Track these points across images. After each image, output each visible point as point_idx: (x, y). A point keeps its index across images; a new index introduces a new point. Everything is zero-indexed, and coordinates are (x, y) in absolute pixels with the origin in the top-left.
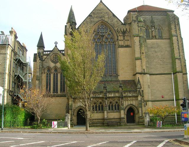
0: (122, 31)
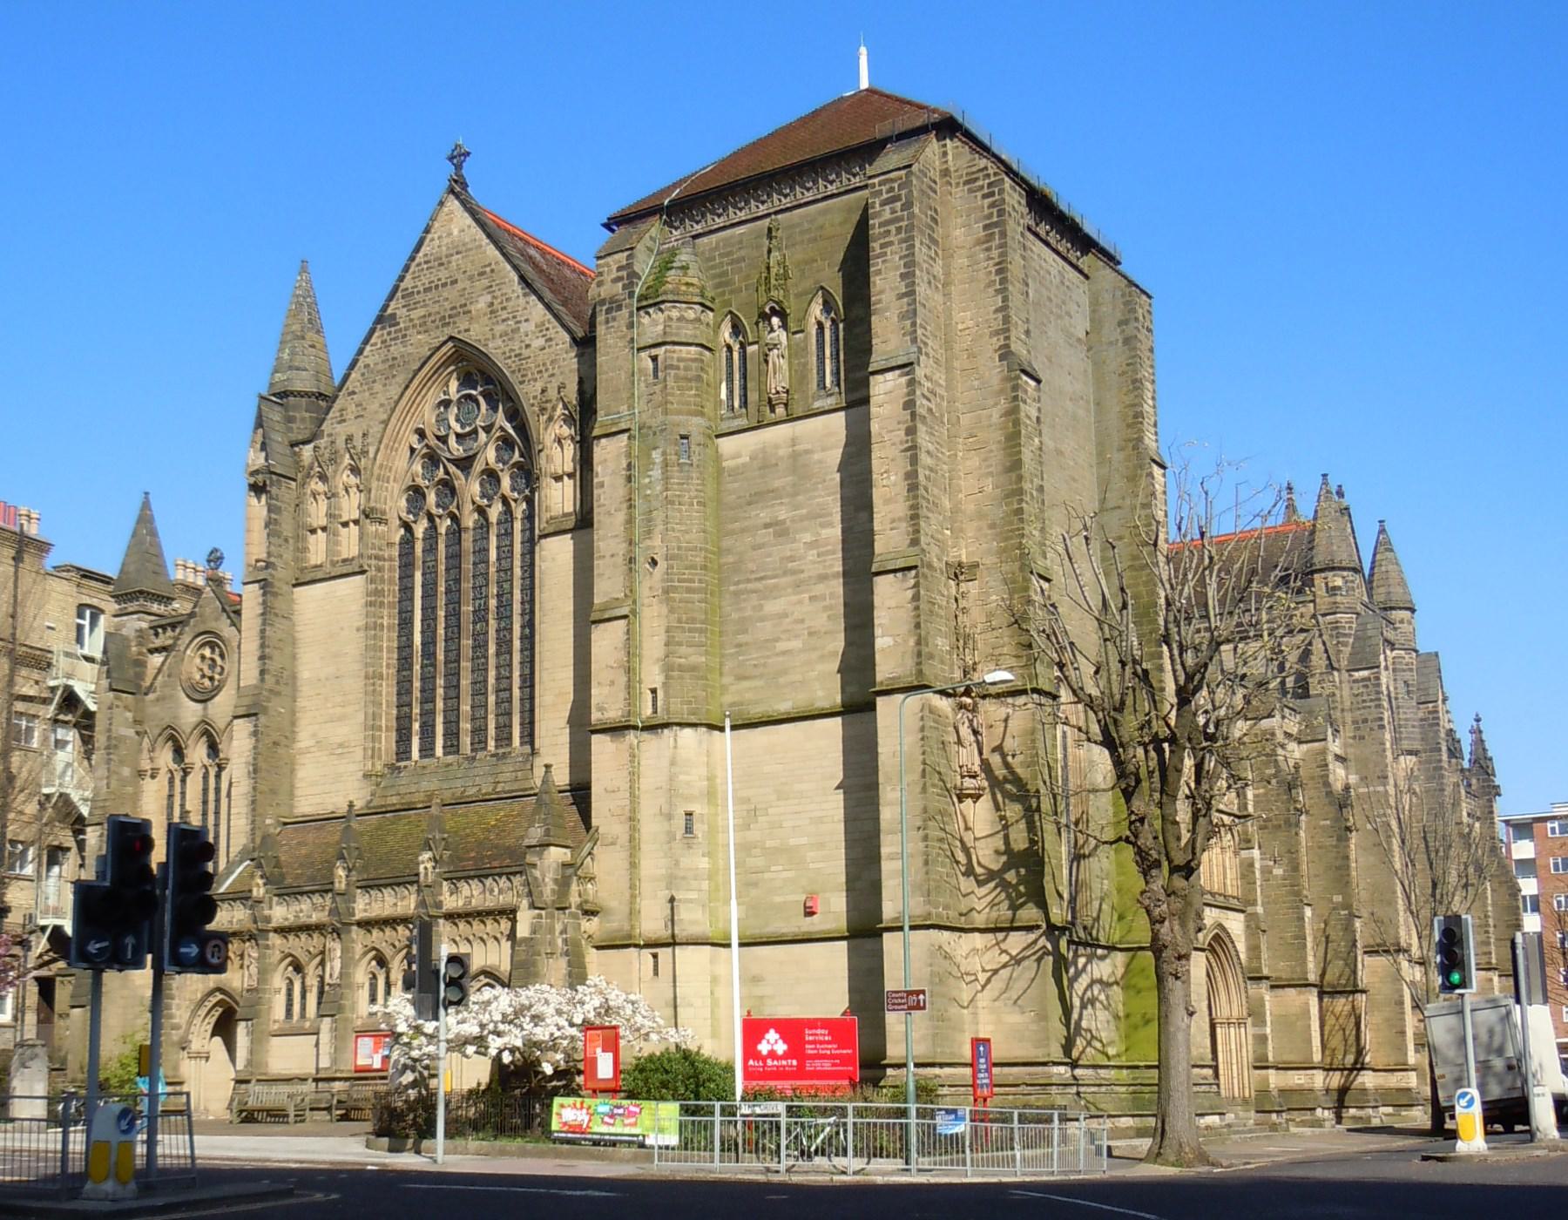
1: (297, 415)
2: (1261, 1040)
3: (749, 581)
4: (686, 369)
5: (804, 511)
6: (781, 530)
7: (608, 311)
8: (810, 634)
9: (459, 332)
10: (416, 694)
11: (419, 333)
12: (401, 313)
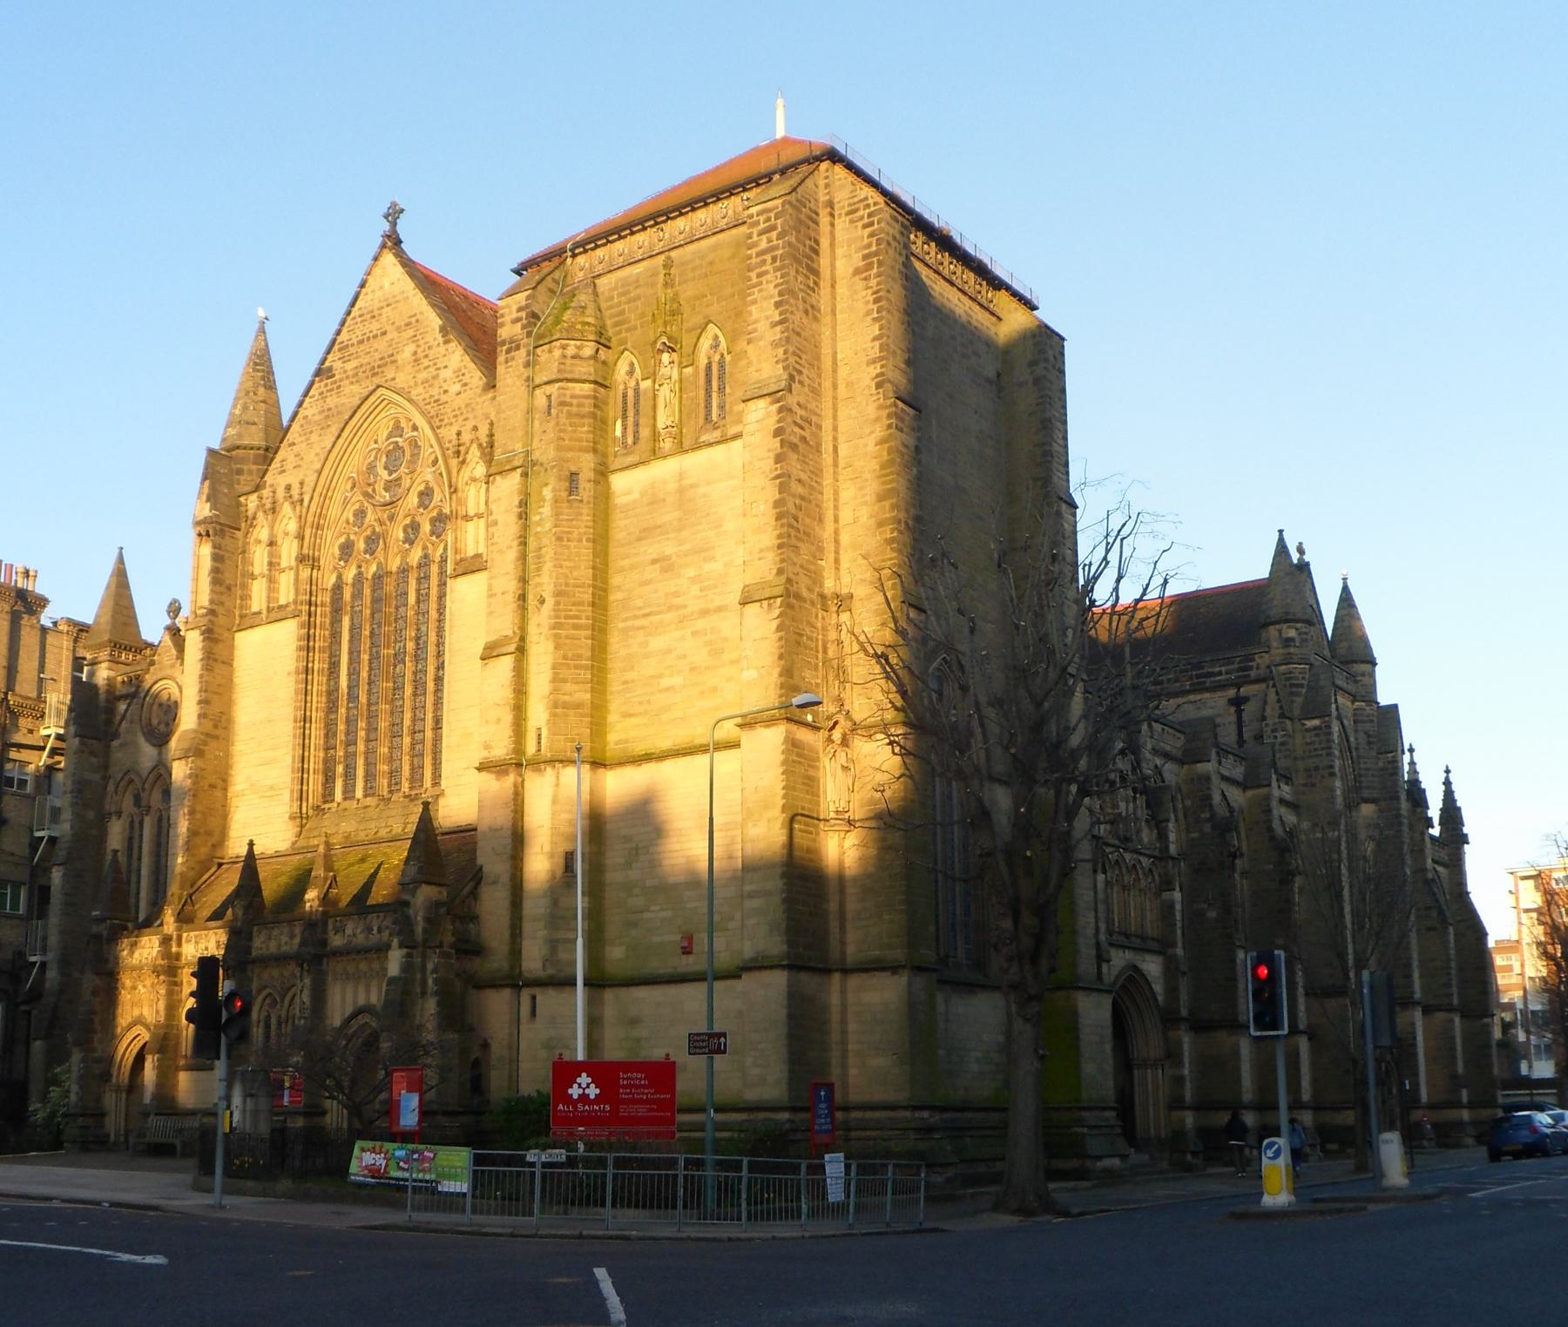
0: (484, 440)
1: (245, 467)
2: (1179, 1080)
3: (636, 617)
4: (580, 405)
5: (688, 546)
6: (665, 565)
7: (508, 351)
8: (692, 669)
9: (386, 381)
10: (341, 736)
11: (352, 383)
12: (338, 365)
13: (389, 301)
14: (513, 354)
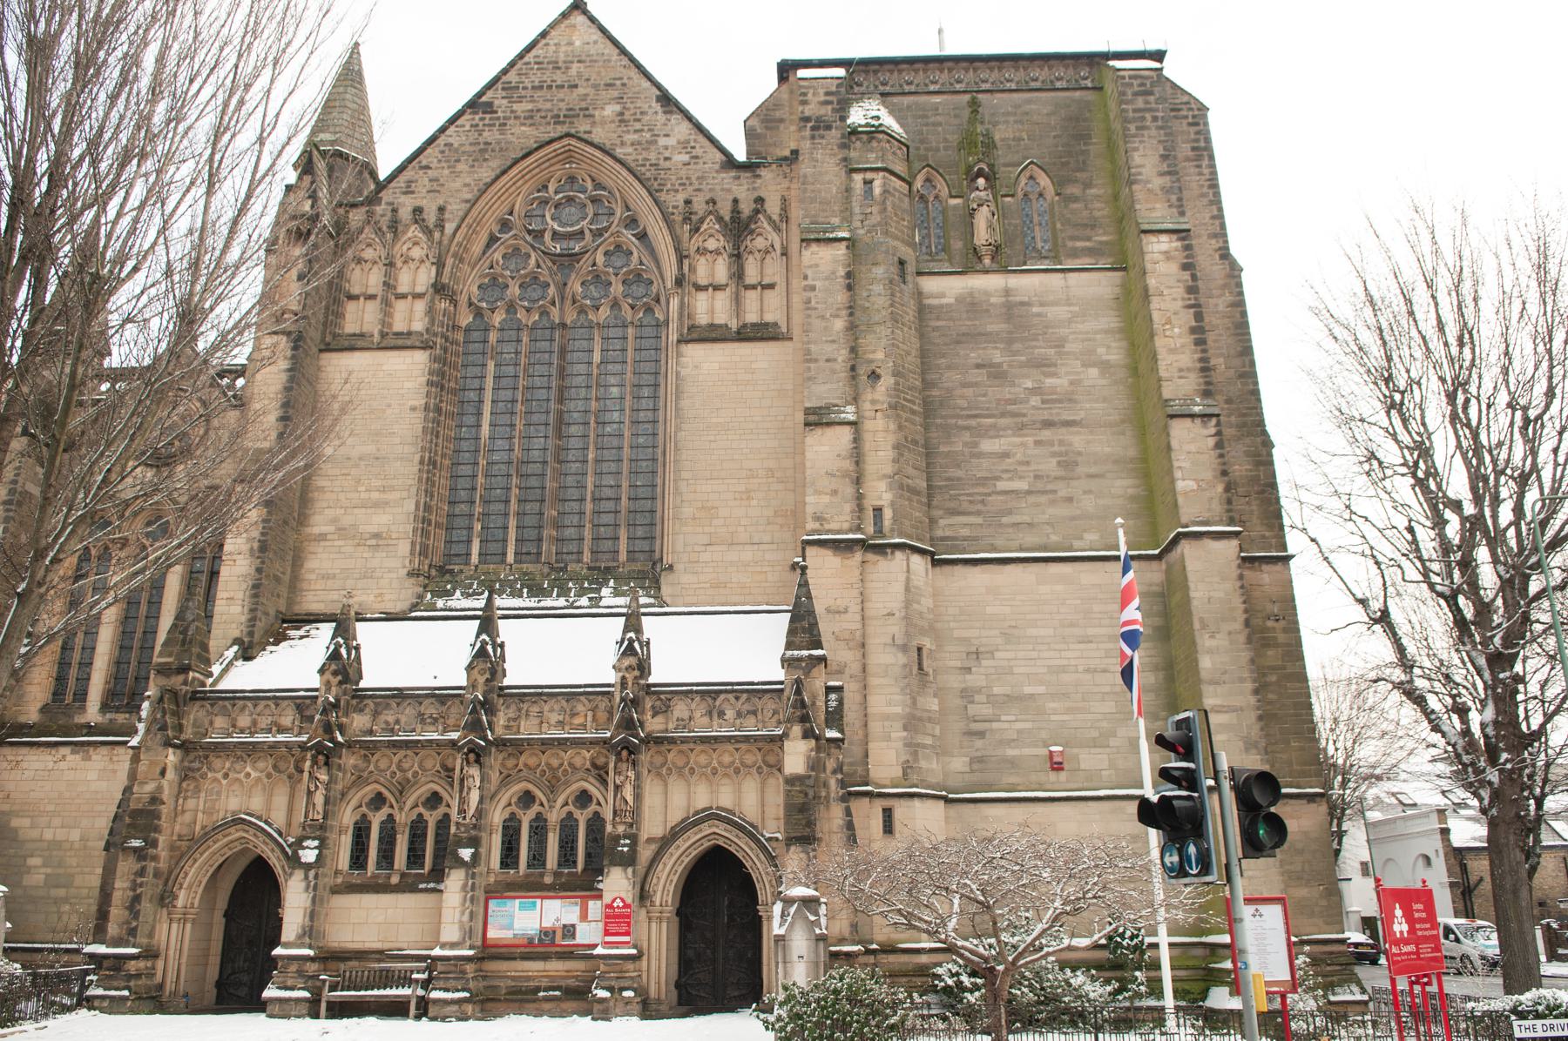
8: (1036, 477)
13: (583, 58)
14: (822, 132)
